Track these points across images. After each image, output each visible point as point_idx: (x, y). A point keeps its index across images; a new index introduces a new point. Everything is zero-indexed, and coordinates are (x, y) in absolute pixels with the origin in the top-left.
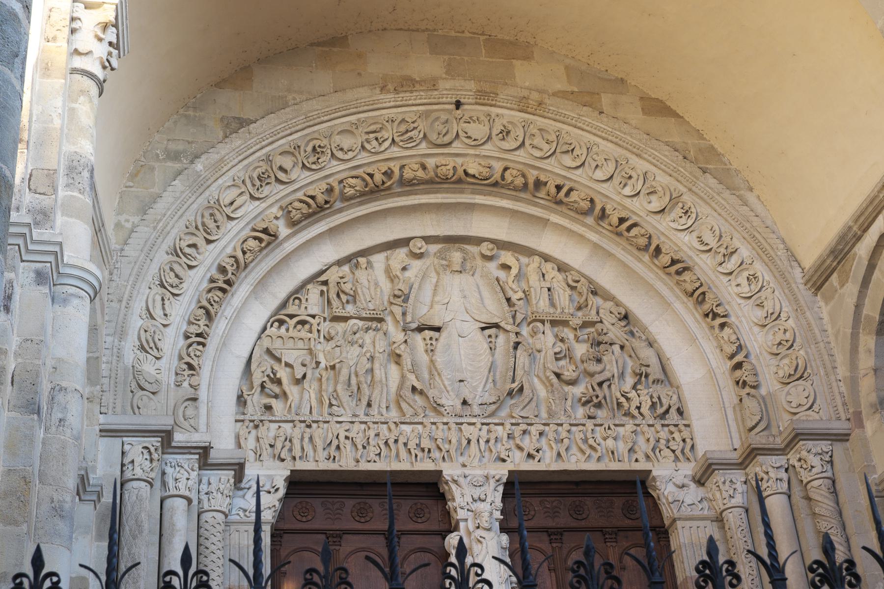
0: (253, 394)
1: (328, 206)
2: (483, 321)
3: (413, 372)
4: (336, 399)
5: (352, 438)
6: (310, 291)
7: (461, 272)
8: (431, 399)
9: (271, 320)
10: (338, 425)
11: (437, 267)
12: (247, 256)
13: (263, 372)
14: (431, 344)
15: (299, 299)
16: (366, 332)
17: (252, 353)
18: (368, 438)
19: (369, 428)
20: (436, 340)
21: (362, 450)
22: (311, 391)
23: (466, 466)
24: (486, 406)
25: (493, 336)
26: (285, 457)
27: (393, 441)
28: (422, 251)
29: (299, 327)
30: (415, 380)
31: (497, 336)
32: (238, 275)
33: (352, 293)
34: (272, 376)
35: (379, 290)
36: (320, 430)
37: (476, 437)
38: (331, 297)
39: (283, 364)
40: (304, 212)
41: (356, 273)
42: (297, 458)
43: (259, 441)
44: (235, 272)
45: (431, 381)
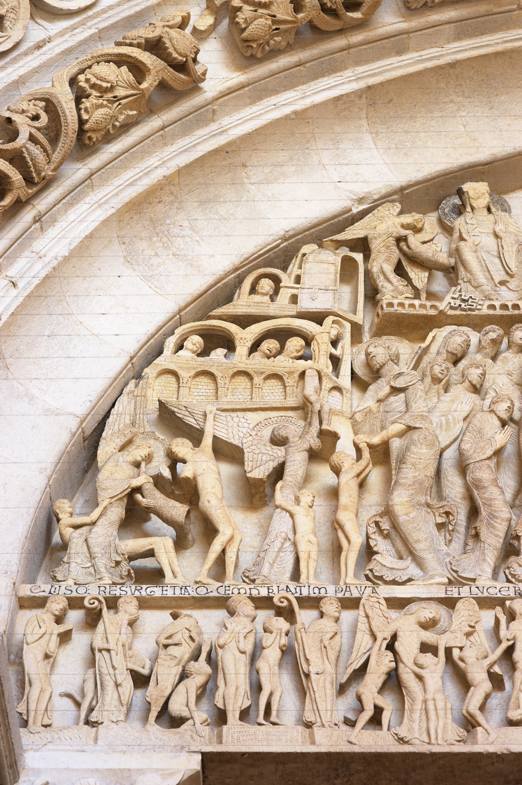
0: (94, 524)
1: (357, 15)
4: (387, 536)
5: (448, 651)
6: (310, 258)
9: (179, 331)
10: (393, 614)
12: (86, 103)
13: (137, 465)
15: (276, 280)
16: (494, 358)
17: (107, 415)
18: (510, 650)
19: (512, 616)
21: (487, 686)
22: (299, 512)
26: (185, 713)
29: (271, 344)
32: (56, 157)
33: (443, 258)
34: (167, 473)
36: (327, 625)
38: (375, 270)
39: (207, 441)
40: (280, 16)
41: (459, 223)
42: (233, 717)
43: (92, 663)
44: (40, 136)
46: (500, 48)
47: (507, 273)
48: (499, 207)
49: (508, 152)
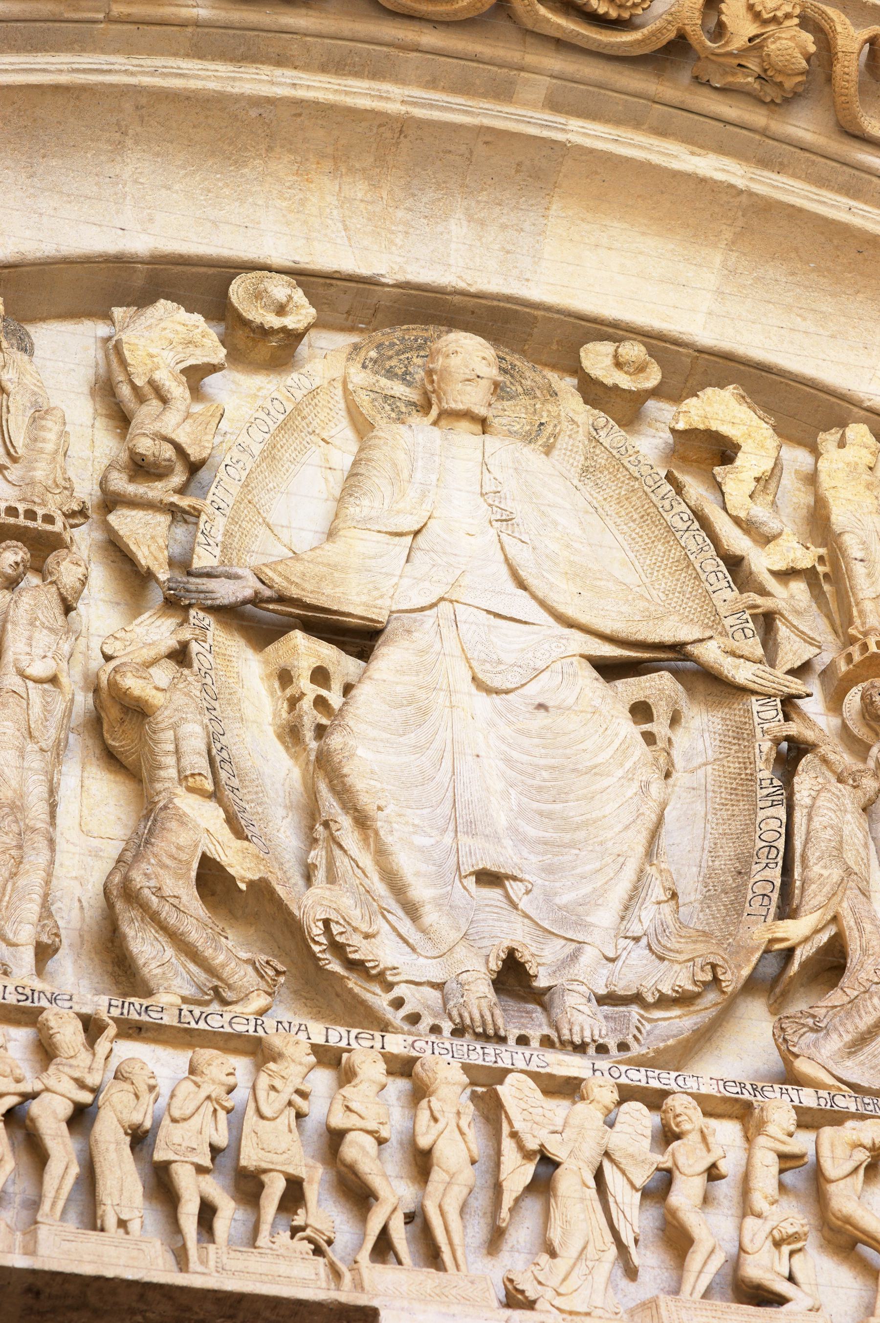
2: (607, 627)
3: (216, 795)
7: (483, 423)
8: (317, 930)
11: (364, 400)
14: (321, 703)
20: (348, 689)
23: (530, 1305)
24: (635, 1010)
25: (661, 713)
27: (65, 1109)
28: (291, 322)
30: (225, 833)
31: (675, 720)
35: (52, 427)
37: (590, 1152)
45: (317, 856)
46: (63, 79)
47: (8, 453)
48: (14, 341)
49: (46, 254)
